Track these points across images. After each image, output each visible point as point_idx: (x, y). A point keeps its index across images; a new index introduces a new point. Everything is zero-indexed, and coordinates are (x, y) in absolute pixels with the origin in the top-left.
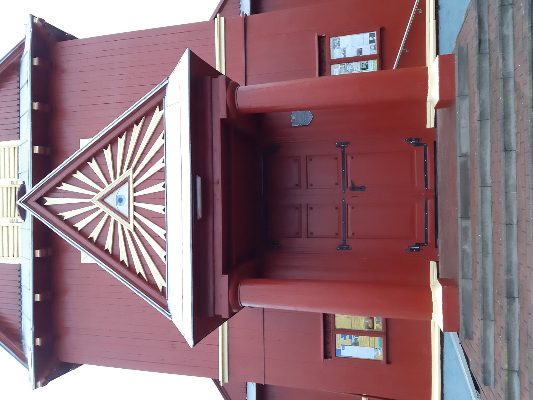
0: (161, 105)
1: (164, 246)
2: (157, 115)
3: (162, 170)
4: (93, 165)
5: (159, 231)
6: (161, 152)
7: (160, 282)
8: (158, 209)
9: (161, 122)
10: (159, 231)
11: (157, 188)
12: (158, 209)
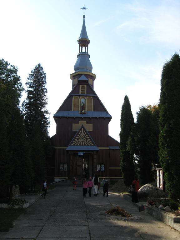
0: (94, 145)
1: (77, 145)
2: (93, 144)
3: (86, 145)
4: (87, 135)
5: (78, 145)
6: (88, 145)
7: (72, 144)
8: (81, 145)
9: (91, 145)
10: (78, 145)
11: (84, 145)
12: (81, 145)
